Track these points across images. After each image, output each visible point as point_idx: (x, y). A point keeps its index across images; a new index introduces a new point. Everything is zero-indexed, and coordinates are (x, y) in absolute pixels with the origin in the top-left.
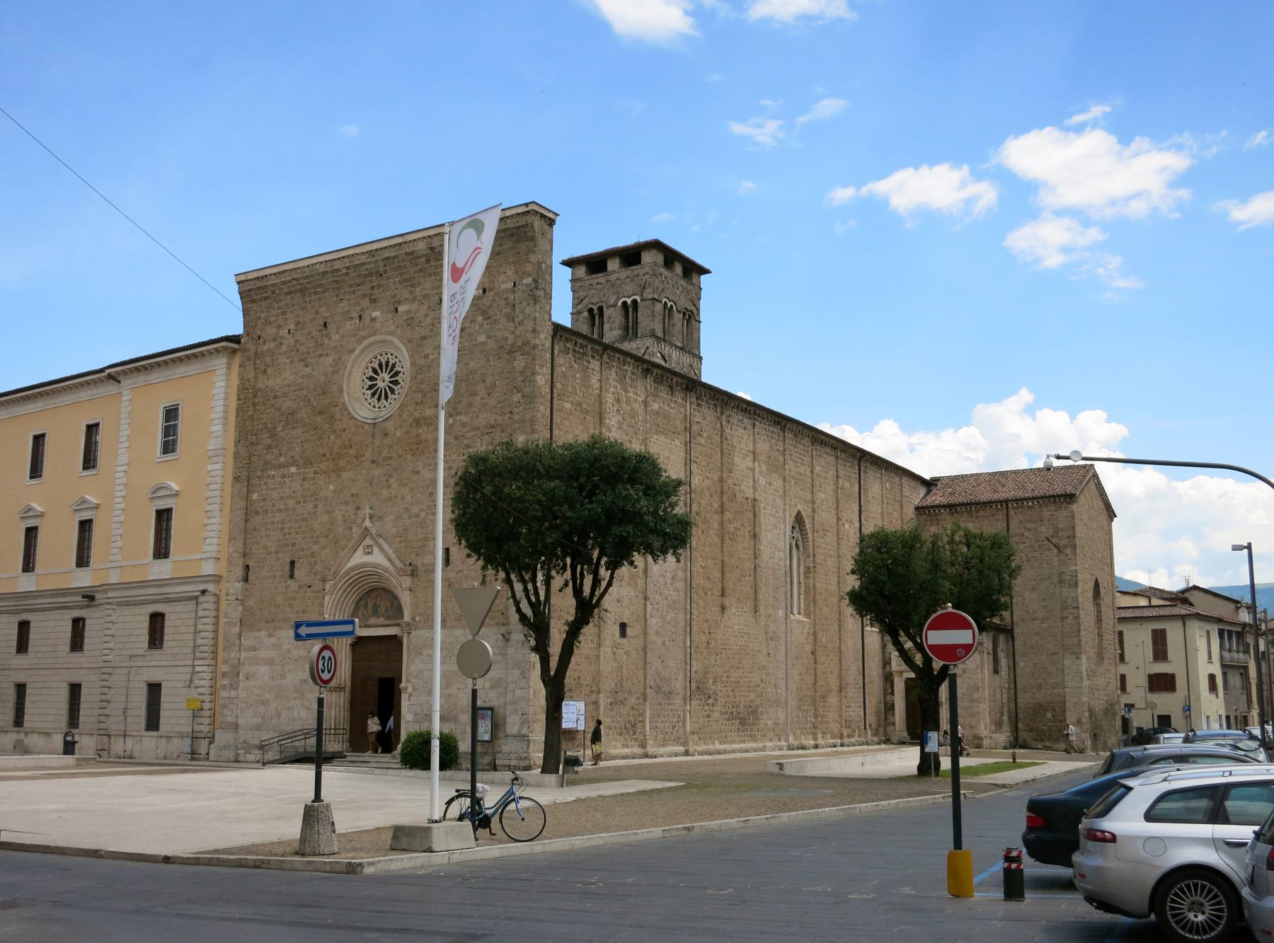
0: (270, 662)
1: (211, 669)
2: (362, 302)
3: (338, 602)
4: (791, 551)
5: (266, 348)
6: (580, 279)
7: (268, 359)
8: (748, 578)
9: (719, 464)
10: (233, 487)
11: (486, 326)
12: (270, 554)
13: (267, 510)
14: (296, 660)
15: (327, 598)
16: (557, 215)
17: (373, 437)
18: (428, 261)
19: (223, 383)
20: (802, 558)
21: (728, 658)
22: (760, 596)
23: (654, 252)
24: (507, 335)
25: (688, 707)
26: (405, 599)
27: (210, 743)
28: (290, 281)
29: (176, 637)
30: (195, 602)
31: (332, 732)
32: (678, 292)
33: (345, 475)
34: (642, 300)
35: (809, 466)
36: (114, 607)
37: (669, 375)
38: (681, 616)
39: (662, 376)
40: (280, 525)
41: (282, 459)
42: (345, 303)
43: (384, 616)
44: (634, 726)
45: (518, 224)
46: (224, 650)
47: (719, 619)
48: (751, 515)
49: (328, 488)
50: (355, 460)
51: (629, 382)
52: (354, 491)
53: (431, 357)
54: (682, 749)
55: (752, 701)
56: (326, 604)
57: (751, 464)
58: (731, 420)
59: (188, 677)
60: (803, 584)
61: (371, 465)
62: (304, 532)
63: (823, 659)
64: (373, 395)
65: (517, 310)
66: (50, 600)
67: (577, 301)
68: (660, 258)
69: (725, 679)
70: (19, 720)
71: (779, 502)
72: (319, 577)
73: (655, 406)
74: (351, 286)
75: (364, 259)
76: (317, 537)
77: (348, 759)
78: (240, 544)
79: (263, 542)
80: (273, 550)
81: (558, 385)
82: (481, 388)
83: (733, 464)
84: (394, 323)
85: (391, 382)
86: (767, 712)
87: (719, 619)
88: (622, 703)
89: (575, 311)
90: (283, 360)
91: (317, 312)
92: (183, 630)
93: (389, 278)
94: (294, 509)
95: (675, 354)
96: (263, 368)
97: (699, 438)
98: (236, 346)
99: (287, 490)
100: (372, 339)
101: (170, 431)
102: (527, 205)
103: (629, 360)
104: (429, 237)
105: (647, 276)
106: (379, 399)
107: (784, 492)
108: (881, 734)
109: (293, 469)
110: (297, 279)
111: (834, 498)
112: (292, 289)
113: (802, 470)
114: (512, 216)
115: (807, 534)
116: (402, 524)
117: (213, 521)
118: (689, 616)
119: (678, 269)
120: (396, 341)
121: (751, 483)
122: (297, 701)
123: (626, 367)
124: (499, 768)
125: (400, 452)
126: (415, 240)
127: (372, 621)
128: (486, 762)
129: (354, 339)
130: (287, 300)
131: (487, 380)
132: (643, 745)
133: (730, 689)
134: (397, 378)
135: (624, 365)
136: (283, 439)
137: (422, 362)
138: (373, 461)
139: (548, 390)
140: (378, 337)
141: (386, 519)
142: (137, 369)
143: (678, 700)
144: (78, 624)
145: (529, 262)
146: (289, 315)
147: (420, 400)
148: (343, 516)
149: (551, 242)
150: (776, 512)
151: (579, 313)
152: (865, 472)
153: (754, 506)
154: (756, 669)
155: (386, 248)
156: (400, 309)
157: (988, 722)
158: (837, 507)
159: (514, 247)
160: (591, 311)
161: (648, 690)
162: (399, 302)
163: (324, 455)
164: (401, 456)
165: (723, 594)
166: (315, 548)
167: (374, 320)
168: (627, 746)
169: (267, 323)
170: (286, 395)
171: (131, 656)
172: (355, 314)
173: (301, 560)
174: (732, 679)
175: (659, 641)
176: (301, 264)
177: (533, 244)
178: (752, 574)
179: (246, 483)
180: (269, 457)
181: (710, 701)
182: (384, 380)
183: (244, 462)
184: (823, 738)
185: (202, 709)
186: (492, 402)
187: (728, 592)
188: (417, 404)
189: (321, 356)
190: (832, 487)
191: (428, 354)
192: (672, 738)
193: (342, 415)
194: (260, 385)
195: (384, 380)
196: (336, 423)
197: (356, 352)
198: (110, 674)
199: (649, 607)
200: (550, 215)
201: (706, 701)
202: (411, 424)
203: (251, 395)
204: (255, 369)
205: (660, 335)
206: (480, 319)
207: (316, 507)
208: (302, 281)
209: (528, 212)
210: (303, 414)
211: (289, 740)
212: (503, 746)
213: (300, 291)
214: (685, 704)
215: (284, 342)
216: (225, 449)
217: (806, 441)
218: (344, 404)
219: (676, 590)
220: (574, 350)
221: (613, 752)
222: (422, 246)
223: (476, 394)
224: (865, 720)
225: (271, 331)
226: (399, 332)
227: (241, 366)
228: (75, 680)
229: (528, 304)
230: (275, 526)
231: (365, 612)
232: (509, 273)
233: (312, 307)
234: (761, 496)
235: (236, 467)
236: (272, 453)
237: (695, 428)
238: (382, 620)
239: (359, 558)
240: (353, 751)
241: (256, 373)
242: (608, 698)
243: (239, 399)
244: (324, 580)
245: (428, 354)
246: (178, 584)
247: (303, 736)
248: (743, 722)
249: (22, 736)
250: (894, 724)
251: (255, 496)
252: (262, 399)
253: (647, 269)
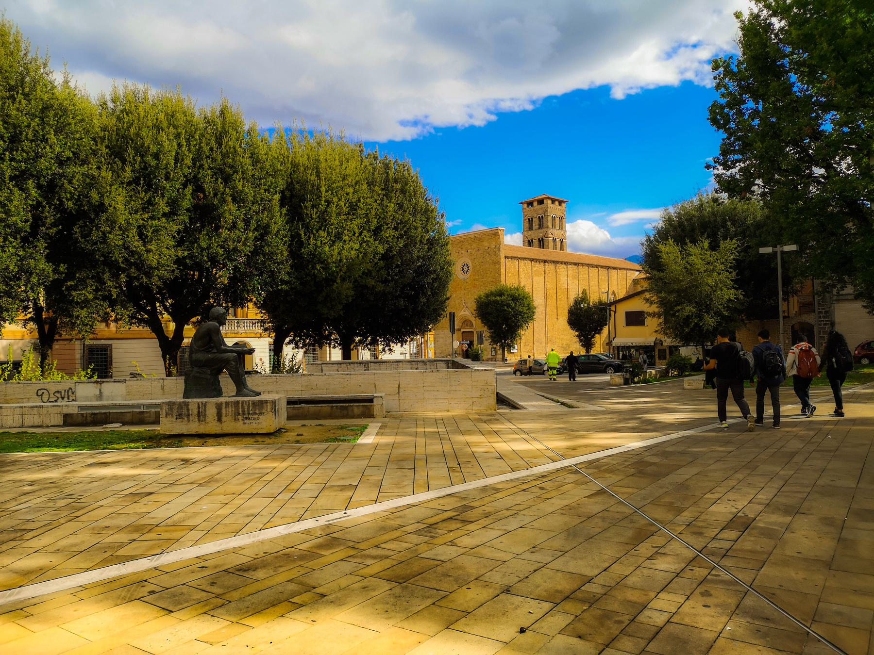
0: (443, 338)
26: (474, 322)
73: (535, 269)
82: (489, 272)
95: (556, 232)
119: (557, 203)
151: (525, 220)
160: (529, 219)
182: (465, 269)
195: (465, 269)
222: (473, 236)
239: (462, 313)
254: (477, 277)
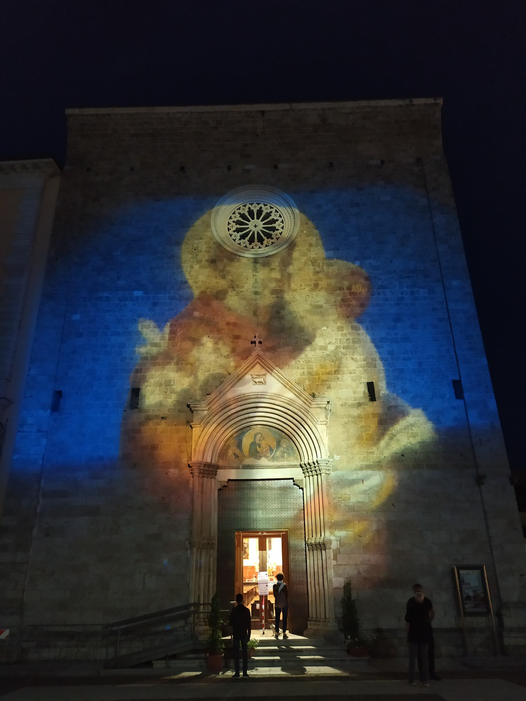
56: (194, 438)
109: (138, 293)
156: (280, 166)
167: (248, 171)
196: (200, 254)
202: (305, 264)
231: (237, 452)
251: (76, 317)
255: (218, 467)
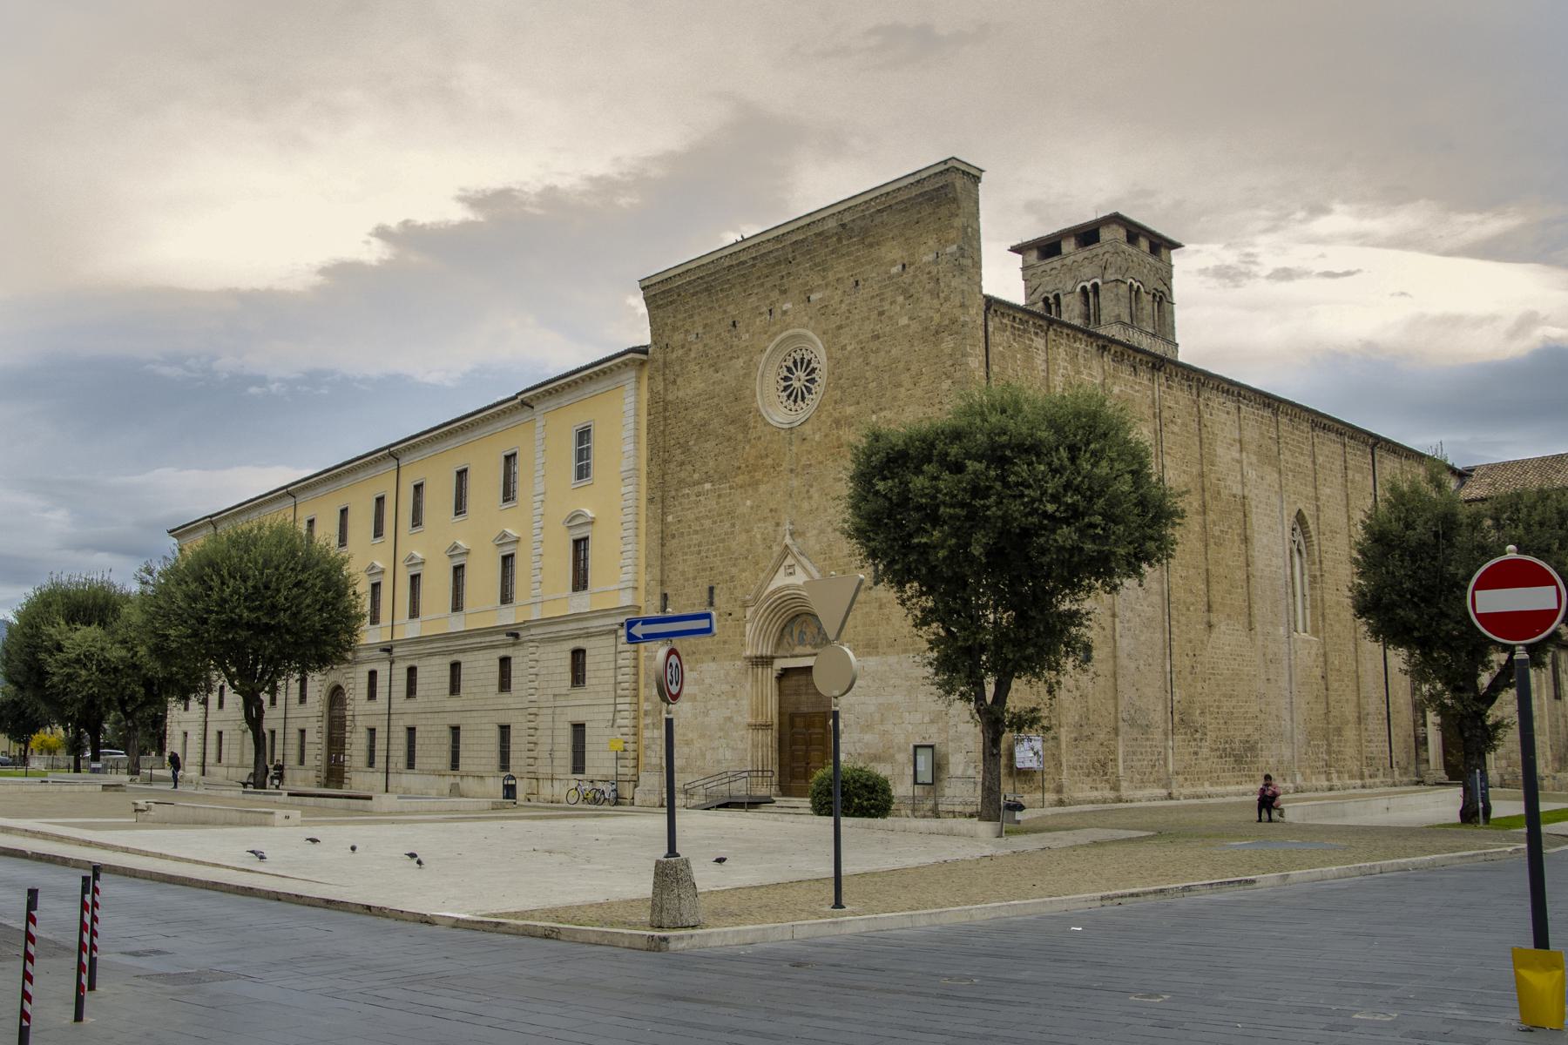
1: (633, 707)
2: (771, 295)
3: (761, 630)
4: (1291, 557)
5: (674, 356)
6: (1032, 266)
7: (677, 368)
8: (1240, 590)
9: (1198, 456)
10: (647, 510)
11: (908, 307)
12: (688, 580)
13: (683, 533)
14: (719, 696)
15: (748, 626)
16: (982, 171)
17: (790, 444)
18: (840, 240)
19: (632, 399)
20: (1306, 566)
21: (1218, 685)
22: (1255, 611)
23: (1115, 227)
24: (931, 314)
25: (1171, 743)
27: (636, 786)
28: (694, 280)
29: (599, 674)
30: (614, 636)
31: (760, 774)
32: (1146, 271)
33: (762, 488)
34: (1104, 283)
35: (1309, 456)
36: (537, 644)
37: (1131, 352)
38: (1158, 635)
39: (1122, 354)
40: (697, 548)
41: (696, 476)
42: (753, 299)
43: (810, 644)
44: (1104, 765)
45: (937, 186)
46: (646, 686)
47: (1205, 638)
48: (1240, 515)
49: (744, 504)
50: (772, 470)
51: (1082, 361)
52: (773, 506)
53: (849, 348)
54: (1164, 792)
55: (1249, 735)
56: (747, 633)
57: (1237, 455)
58: (1211, 404)
59: (610, 716)
60: (1308, 597)
61: (790, 475)
62: (722, 555)
63: (1336, 685)
64: (789, 397)
65: (942, 284)
66: (479, 640)
67: (1030, 291)
68: (1121, 233)
69: (1216, 710)
70: (455, 764)
71: (1275, 500)
72: (739, 603)
74: (759, 278)
75: (770, 247)
76: (736, 559)
77: (777, 804)
78: (657, 571)
79: (680, 568)
80: (691, 576)
81: (995, 369)
83: (1215, 455)
84: (807, 314)
85: (807, 381)
86: (1269, 749)
87: (1205, 638)
88: (1088, 738)
89: (1028, 302)
90: (693, 367)
91: (725, 312)
92: (604, 666)
93: (798, 264)
94: (711, 529)
96: (672, 378)
97: (1171, 425)
98: (643, 357)
99: (703, 510)
100: (784, 334)
101: (583, 455)
102: (945, 162)
103: (1080, 336)
104: (839, 212)
105: (1107, 256)
106: (795, 401)
107: (1281, 486)
108: (1412, 774)
109: (708, 486)
110: (701, 278)
111: (1343, 494)
112: (698, 289)
113: (1301, 460)
114: (930, 176)
115: (1311, 537)
116: (825, 539)
117: (629, 547)
118: (1168, 636)
119: (1144, 244)
120: (810, 334)
121: (1239, 478)
122: (722, 740)
123: (1077, 345)
124: (942, 814)
125: (820, 458)
126: (824, 218)
127: (798, 650)
128: (928, 807)
129: (766, 336)
130: (693, 302)
131: (912, 367)
132: (1115, 788)
133: (1222, 721)
134: (814, 376)
135: (1075, 342)
136: (696, 453)
137: (839, 355)
138: (792, 471)
139: (983, 374)
140: (790, 332)
141: (808, 535)
142: (549, 392)
143: (1158, 735)
144: (505, 662)
145: (952, 227)
146: (696, 318)
147: (838, 397)
148: (763, 534)
149: (977, 202)
150: (1272, 511)
152: (1379, 461)
153: (1244, 505)
154: (1254, 698)
155: (793, 231)
156: (813, 297)
157: (1550, 758)
158: (1348, 505)
159: (934, 213)
160: (1046, 300)
161: (1121, 724)
162: (811, 291)
163: (739, 468)
164: (821, 463)
165: (1209, 610)
166: (734, 571)
167: (785, 313)
168: (1097, 789)
169: (675, 329)
170: (696, 405)
171: (555, 695)
172: (765, 309)
173: (720, 586)
174: (1225, 709)
175: (1133, 666)
176: (704, 261)
177: (955, 206)
178: (1245, 586)
179: (660, 506)
180: (683, 475)
181: (1198, 736)
183: (657, 482)
184: (1339, 778)
185: (625, 751)
186: (919, 392)
187: (1215, 607)
188: (836, 403)
189: (731, 359)
190: (1340, 480)
191: (845, 345)
192: (1152, 779)
193: (755, 422)
194: (670, 397)
197: (768, 351)
198: (536, 715)
199: (1118, 627)
200: (973, 172)
201: (1192, 735)
203: (661, 409)
204: (664, 380)
205: (1127, 320)
206: (900, 299)
207: (733, 525)
208: (707, 279)
209: (948, 170)
210: (715, 424)
211: (715, 783)
212: (946, 790)
213: (706, 289)
214: (1167, 739)
215: (692, 347)
216: (638, 470)
217: (1305, 426)
218: (758, 410)
219: (1151, 605)
220: (1013, 327)
221: (1079, 795)
223: (900, 385)
224: (1391, 757)
225: (678, 337)
226: (812, 323)
227: (650, 378)
228: (505, 721)
229: (954, 276)
230: (692, 549)
231: (790, 640)
232: (931, 243)
233: (720, 307)
234: (1251, 493)
235: (649, 488)
236: (685, 470)
237: (1165, 414)
238: (809, 650)
239: (780, 580)
240: (784, 795)
241: (666, 385)
242: (1072, 732)
243: (649, 414)
244: (745, 606)
245: (845, 345)
246: (597, 617)
247: (727, 780)
248: (1239, 760)
249: (458, 780)
250: (1428, 761)
251: (670, 519)
252: (673, 413)
253: (1107, 247)
254: (850, 410)
255: (773, 658)
